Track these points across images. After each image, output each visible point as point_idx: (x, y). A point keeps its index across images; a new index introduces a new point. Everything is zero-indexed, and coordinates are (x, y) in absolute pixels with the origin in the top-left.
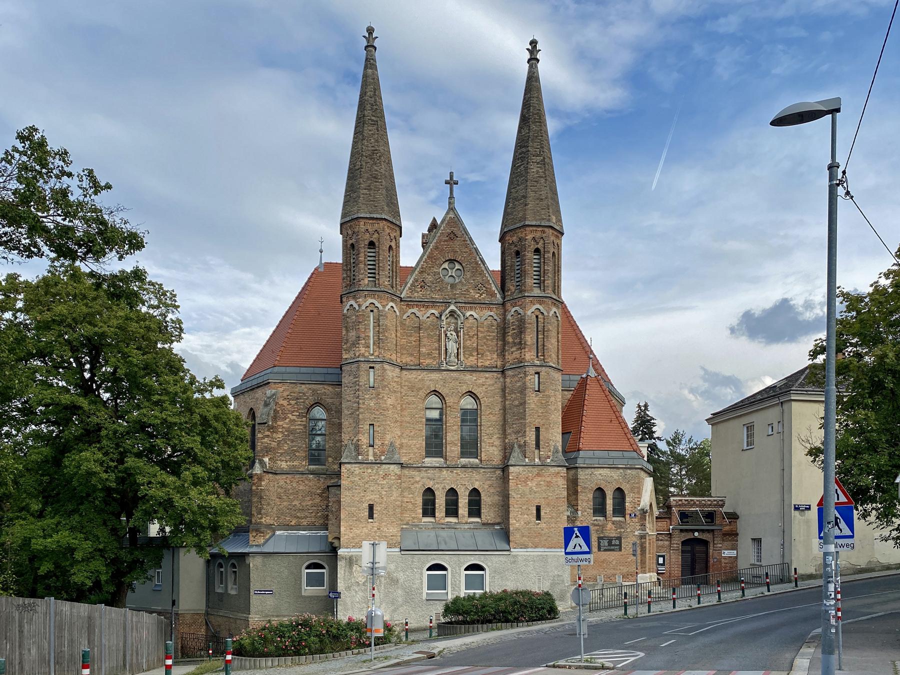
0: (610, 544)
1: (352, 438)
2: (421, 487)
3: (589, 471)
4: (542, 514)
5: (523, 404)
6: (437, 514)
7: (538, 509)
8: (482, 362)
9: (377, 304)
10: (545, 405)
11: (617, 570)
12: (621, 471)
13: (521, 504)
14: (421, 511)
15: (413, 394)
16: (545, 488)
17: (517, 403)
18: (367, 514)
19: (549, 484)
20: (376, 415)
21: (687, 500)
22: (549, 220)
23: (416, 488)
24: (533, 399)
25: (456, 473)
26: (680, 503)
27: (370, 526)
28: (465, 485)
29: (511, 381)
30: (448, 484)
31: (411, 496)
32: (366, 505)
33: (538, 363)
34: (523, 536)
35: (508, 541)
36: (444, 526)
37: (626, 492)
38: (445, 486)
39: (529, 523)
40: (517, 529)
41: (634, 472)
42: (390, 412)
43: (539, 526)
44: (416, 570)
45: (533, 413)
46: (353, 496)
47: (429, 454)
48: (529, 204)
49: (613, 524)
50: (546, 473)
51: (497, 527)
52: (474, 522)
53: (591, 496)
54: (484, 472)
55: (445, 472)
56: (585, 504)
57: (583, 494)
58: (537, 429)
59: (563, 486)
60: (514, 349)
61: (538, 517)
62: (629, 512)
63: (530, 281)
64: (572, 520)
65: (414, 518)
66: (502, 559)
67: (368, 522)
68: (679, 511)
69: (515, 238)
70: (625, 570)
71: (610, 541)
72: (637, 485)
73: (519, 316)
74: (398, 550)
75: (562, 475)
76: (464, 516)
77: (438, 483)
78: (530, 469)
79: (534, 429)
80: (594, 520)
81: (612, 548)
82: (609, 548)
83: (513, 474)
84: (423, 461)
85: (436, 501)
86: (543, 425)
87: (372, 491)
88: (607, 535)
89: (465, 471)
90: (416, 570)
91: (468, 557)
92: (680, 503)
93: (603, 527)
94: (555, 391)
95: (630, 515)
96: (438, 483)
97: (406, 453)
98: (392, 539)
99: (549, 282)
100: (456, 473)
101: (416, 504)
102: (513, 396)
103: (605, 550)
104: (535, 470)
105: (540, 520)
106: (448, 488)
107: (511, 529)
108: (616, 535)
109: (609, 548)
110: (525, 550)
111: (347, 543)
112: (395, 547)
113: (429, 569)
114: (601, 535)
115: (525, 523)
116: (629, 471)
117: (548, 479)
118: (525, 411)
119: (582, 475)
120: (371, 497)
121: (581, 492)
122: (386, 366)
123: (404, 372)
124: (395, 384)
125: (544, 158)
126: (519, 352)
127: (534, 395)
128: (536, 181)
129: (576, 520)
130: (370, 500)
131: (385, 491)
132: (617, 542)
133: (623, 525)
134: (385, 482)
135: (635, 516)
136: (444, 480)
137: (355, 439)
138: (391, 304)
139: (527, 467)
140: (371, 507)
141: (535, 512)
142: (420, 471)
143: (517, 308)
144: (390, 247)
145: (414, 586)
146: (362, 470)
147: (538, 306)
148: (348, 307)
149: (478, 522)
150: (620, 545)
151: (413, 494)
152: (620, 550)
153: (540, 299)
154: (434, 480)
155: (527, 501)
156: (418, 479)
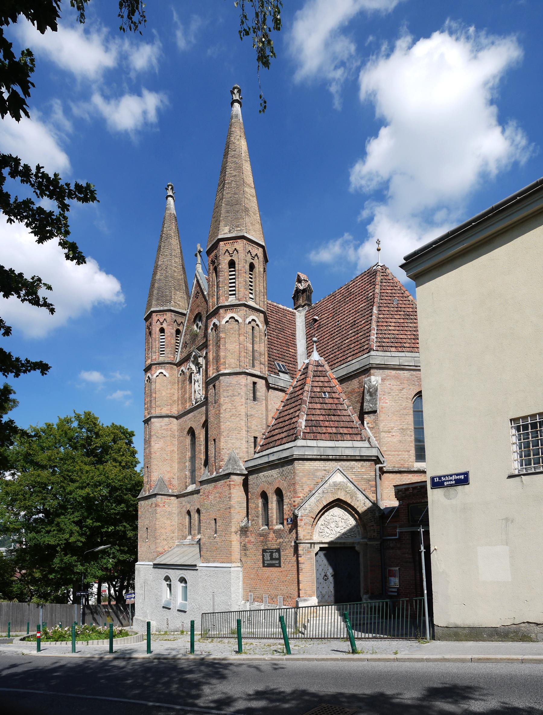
42: (157, 455)
43: (215, 540)
49: (274, 533)
81: (274, 562)
82: (270, 562)
129: (247, 531)
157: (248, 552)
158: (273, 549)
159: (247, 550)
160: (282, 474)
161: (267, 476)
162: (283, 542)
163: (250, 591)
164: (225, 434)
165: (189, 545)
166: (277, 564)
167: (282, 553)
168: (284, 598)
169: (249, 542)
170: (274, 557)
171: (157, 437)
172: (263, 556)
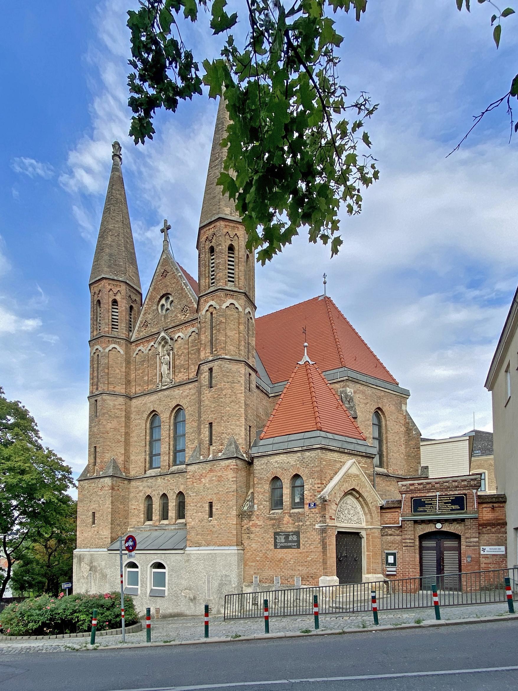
3: (264, 460)
6: (153, 518)
7: (211, 505)
11: (295, 570)
12: (299, 454)
13: (196, 502)
16: (216, 483)
19: (220, 479)
23: (140, 496)
24: (207, 396)
28: (173, 489)
30: (161, 490)
31: (137, 503)
32: (90, 513)
34: (197, 535)
36: (157, 528)
38: (159, 492)
39: (202, 520)
40: (193, 528)
41: (313, 454)
43: (210, 524)
45: (206, 409)
49: (290, 516)
55: (159, 480)
56: (261, 496)
57: (260, 486)
62: (308, 502)
64: (248, 515)
65: (138, 522)
67: (92, 527)
70: (304, 571)
71: (287, 536)
72: (317, 469)
75: (232, 467)
76: (172, 518)
77: (154, 490)
78: (204, 465)
81: (290, 544)
82: (286, 544)
83: (190, 473)
85: (153, 506)
89: (174, 477)
91: (153, 556)
93: (279, 520)
95: (310, 506)
96: (154, 490)
97: (134, 467)
98: (105, 541)
100: (168, 480)
101: (140, 510)
103: (282, 547)
104: (208, 466)
106: (161, 493)
110: (197, 548)
111: (80, 544)
114: (278, 530)
115: (199, 521)
116: (307, 454)
117: (219, 474)
122: (105, 397)
127: (207, 392)
129: (252, 515)
131: (102, 501)
132: (295, 538)
135: (314, 505)
136: (158, 487)
139: (201, 464)
141: (207, 509)
142: (143, 482)
150: (298, 542)
151: (138, 502)
152: (298, 547)
154: (152, 488)
155: (201, 499)
156: (141, 488)
157: (252, 536)
159: (251, 533)
161: (282, 463)
162: (302, 525)
169: (256, 525)
172: (275, 539)
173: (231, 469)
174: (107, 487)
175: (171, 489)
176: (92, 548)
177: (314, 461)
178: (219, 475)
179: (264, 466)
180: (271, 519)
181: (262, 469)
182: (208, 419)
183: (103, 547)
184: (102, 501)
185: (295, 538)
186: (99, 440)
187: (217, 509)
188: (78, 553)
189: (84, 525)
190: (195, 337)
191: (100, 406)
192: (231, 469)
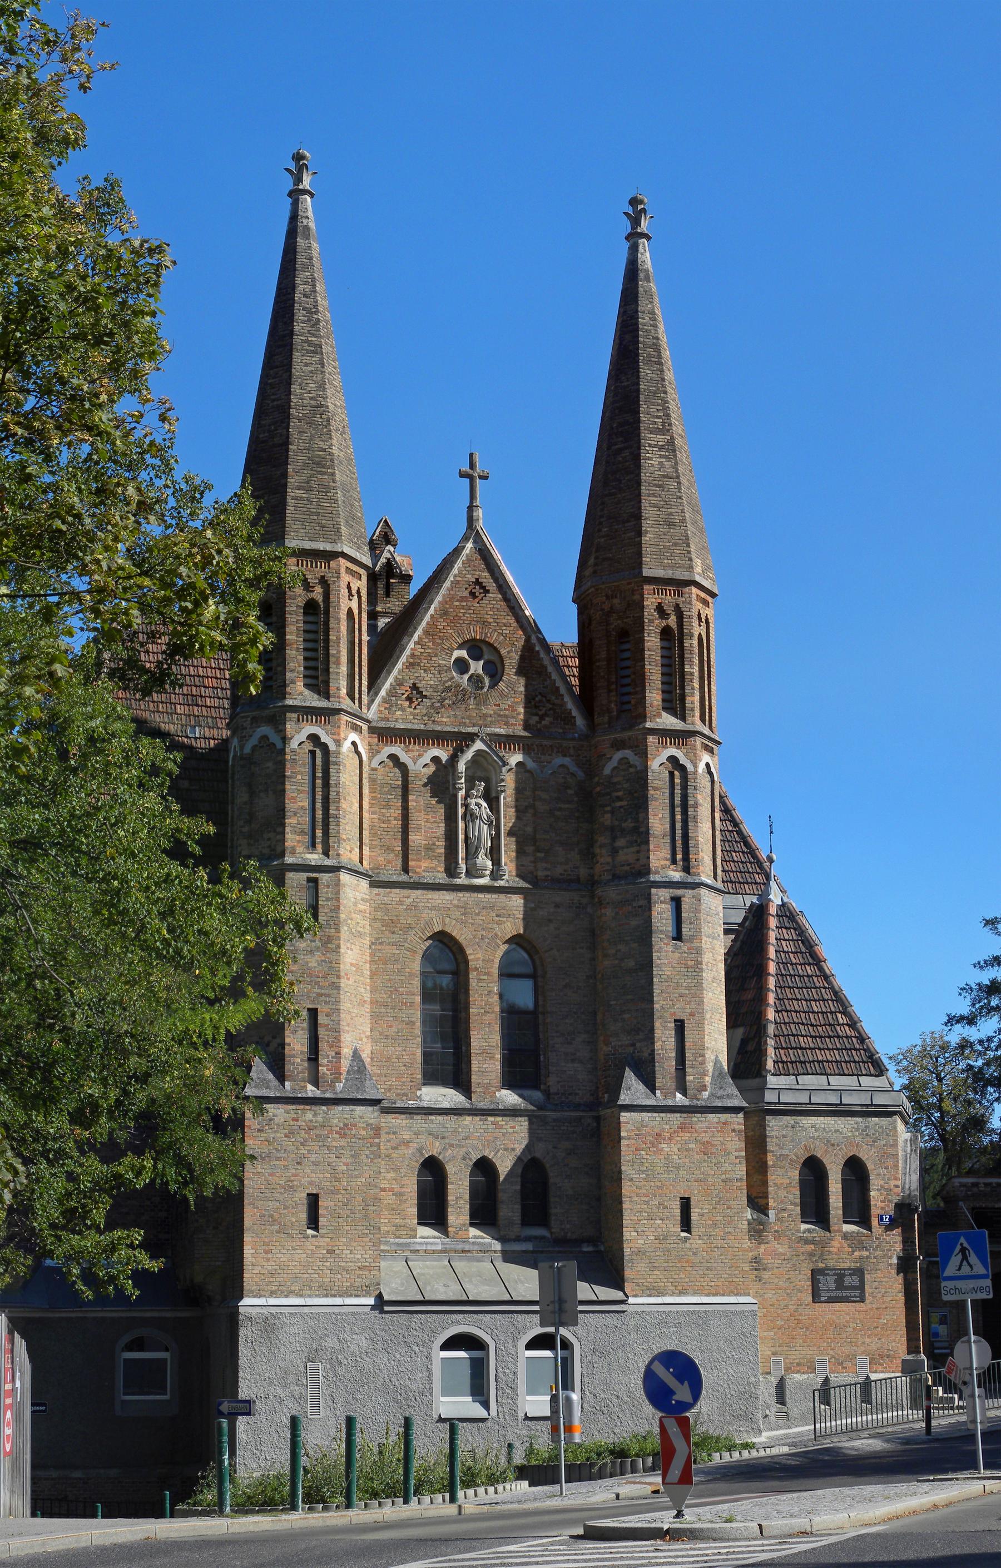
0: (840, 1285)
1: (267, 1039)
2: (413, 1155)
4: (694, 1217)
5: (646, 966)
7: (686, 1205)
8: (546, 869)
9: (324, 738)
10: (695, 968)
14: (414, 1211)
15: (395, 938)
17: (631, 963)
18: (304, 1216)
20: (320, 987)
21: (990, 1184)
22: (691, 568)
25: (493, 1123)
26: (975, 1190)
27: (310, 1245)
29: (617, 913)
31: (393, 1174)
32: (301, 1197)
33: (676, 875)
35: (618, 1283)
37: (870, 1166)
39: (665, 1238)
40: (639, 1252)
42: (350, 983)
43: (687, 1245)
44: (416, 1349)
46: (271, 1175)
47: (432, 1076)
48: (647, 532)
50: (700, 1125)
51: (586, 1248)
52: (536, 1238)
53: (795, 1175)
54: (555, 1120)
56: (783, 1193)
57: (780, 1171)
58: (680, 1026)
59: (737, 1154)
60: (620, 842)
61: (686, 1224)
62: (879, 1211)
63: (654, 697)
65: (398, 1227)
66: (610, 1320)
68: (973, 1209)
69: (616, 601)
71: (840, 1276)
73: (632, 770)
74: (371, 1301)
75: (737, 1127)
77: (451, 1145)
79: (673, 1025)
80: (804, 1232)
81: (845, 1293)
82: (839, 1293)
84: (419, 1093)
86: (692, 1014)
87: (315, 1164)
88: (831, 1263)
90: (416, 1349)
92: (975, 1190)
93: (823, 1244)
94: (713, 938)
96: (451, 1145)
99: (693, 700)
102: (622, 947)
103: (831, 1300)
105: (689, 1231)
106: (475, 1156)
107: (627, 1251)
108: (853, 1265)
109: (839, 1293)
112: (367, 1294)
113: (445, 1346)
114: (821, 1265)
118: (651, 983)
119: (775, 1125)
120: (310, 1180)
121: (774, 1166)
122: (344, 877)
123: (376, 890)
124: (358, 917)
125: (672, 438)
126: (634, 849)
127: (670, 948)
128: (659, 486)
130: (311, 1183)
131: (346, 1164)
132: (855, 1281)
133: (867, 1243)
134: (343, 1142)
136: (466, 1138)
137: (274, 1045)
138: (353, 736)
140: (313, 1200)
141: (678, 1212)
142: (412, 1118)
143: (627, 753)
144: (350, 611)
145: (414, 1387)
146: (293, 1115)
147: (673, 751)
148: (253, 741)
149: (542, 1238)
150: (861, 1287)
152: (862, 1300)
153: (681, 737)
154: (443, 1138)
155: (660, 1188)
156: (407, 1135)
157: (766, 1275)
158: (844, 1269)
159: (764, 1269)
160: (865, 1132)
161: (824, 1129)
162: (868, 1257)
163: (774, 1354)
164: (708, 1016)
165: (441, 1251)
166: (855, 1296)
167: (867, 1277)
168: (871, 1359)
169: (776, 1254)
170: (846, 1284)
171: (350, 930)
173: (733, 1130)
174: (364, 1129)
175: (505, 1149)
176: (310, 1296)
177: (887, 1135)
178: (705, 1139)
179: (788, 1132)
180: (807, 1242)
181: (784, 1136)
182: (672, 1011)
183: (353, 1292)
184: (346, 1164)
185: (855, 1281)
186: (329, 996)
187: (702, 1215)
188: (258, 1310)
189: (276, 1227)
190: (565, 778)
191: (328, 899)
192: (733, 1130)
